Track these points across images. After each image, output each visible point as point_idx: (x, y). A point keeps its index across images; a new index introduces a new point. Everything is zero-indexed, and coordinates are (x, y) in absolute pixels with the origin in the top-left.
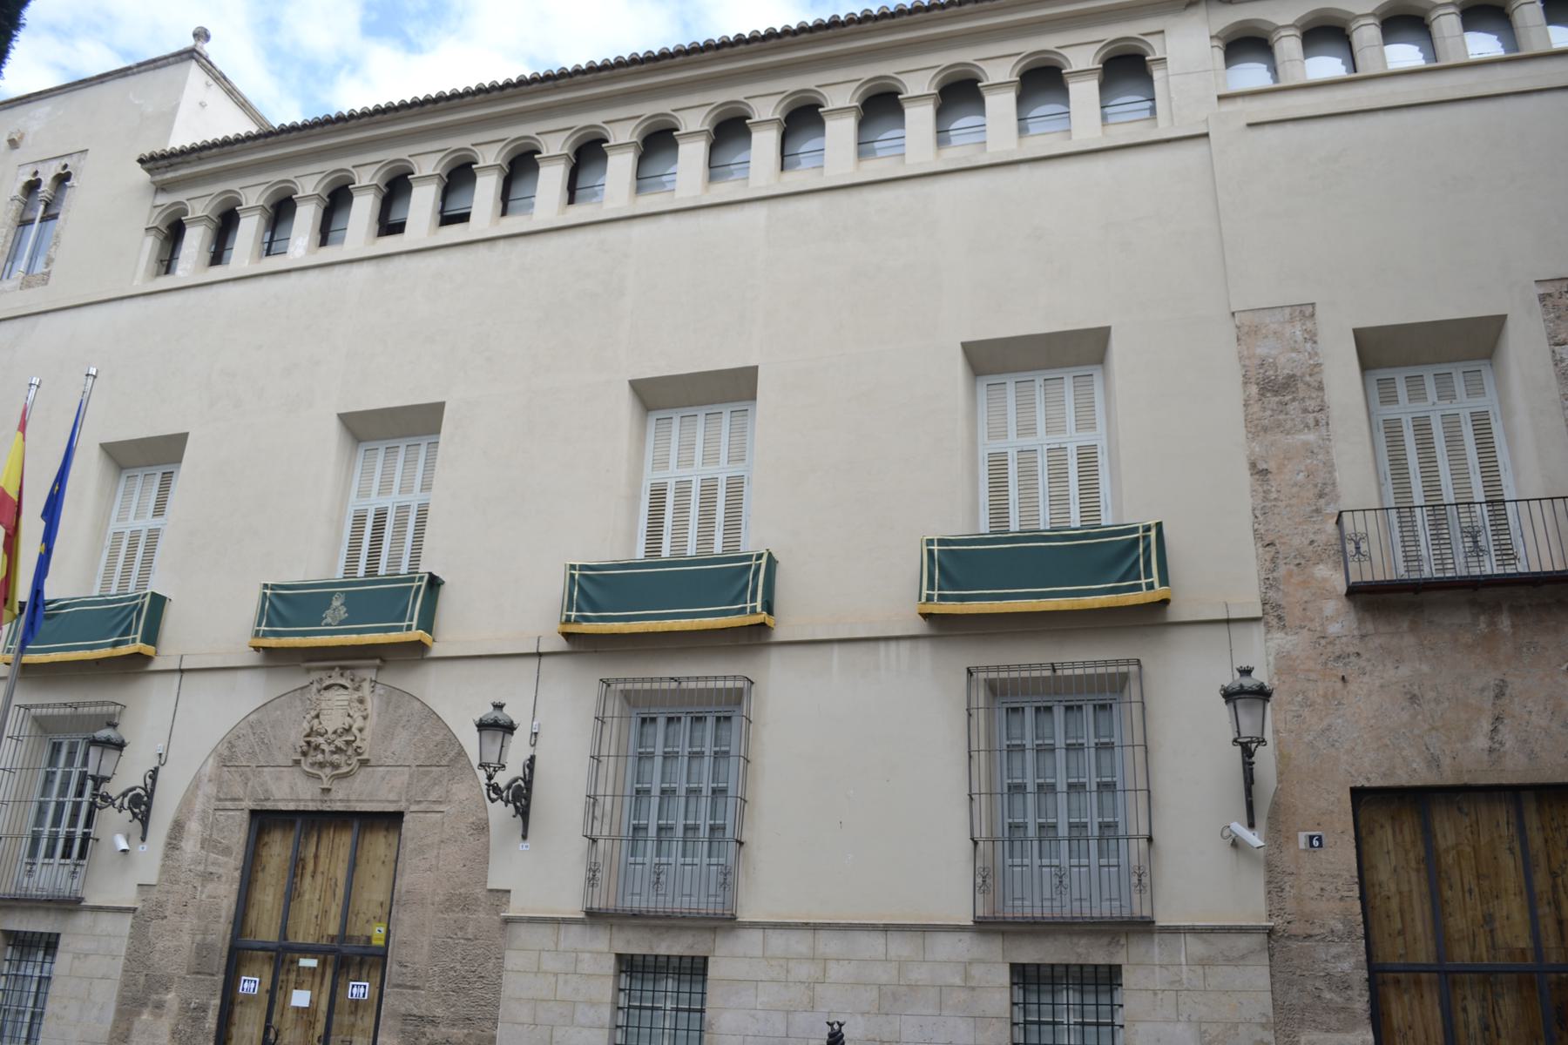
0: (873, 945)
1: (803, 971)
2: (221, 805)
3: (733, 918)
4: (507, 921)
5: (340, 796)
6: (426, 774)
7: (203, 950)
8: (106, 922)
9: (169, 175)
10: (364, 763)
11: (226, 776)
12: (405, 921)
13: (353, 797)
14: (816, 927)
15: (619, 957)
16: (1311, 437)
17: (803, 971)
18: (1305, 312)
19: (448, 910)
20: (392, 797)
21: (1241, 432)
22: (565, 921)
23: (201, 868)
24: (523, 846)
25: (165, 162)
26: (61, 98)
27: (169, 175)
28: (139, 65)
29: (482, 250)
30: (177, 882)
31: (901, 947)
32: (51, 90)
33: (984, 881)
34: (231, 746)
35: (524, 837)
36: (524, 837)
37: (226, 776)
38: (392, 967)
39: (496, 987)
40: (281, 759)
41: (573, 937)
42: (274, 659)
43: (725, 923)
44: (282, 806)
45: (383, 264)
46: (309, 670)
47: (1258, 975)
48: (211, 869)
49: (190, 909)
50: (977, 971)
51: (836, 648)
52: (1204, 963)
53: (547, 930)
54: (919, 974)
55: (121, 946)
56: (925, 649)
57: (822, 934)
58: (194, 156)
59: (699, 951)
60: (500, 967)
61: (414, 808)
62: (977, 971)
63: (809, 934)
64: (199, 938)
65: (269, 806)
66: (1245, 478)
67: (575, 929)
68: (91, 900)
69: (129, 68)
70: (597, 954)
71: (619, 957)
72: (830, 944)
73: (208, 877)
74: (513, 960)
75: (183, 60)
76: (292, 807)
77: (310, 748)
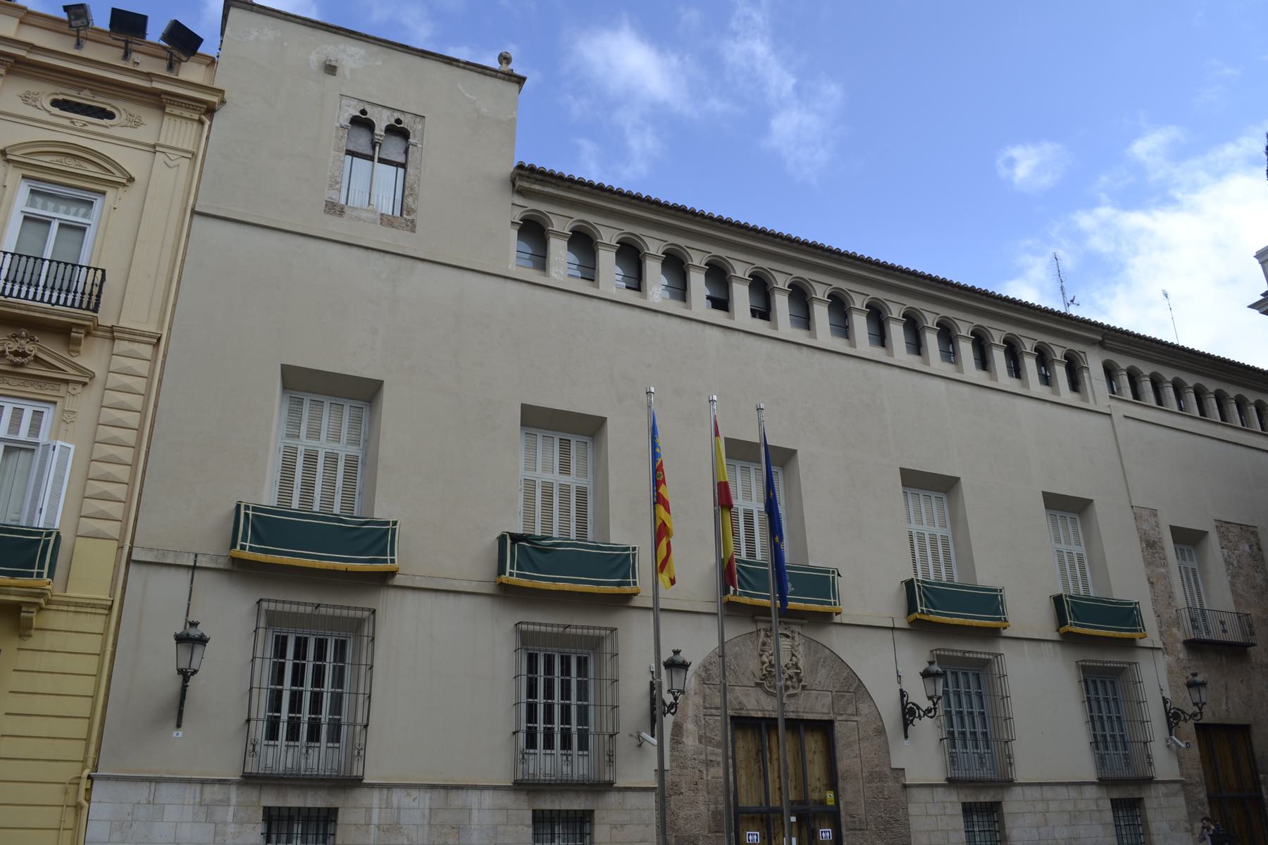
0: (1062, 791)
1: (1040, 806)
2: (709, 712)
3: (1012, 781)
4: (905, 786)
5: (792, 709)
6: (843, 697)
7: (715, 814)
8: (633, 800)
9: (537, 187)
10: (804, 687)
11: (708, 691)
12: (849, 790)
13: (801, 710)
14: (1041, 784)
15: (964, 804)
16: (1163, 570)
17: (1040, 806)
18: (1154, 513)
19: (871, 781)
20: (825, 710)
21: (1142, 565)
22: (937, 786)
23: (703, 757)
24: (906, 743)
25: (540, 177)
26: (375, 48)
27: (537, 187)
28: (468, 63)
29: (779, 345)
30: (685, 767)
31: (1073, 793)
32: (366, 36)
33: (1101, 762)
34: (706, 670)
35: (906, 737)
36: (906, 737)
37: (708, 691)
38: (844, 819)
39: (907, 826)
40: (746, 682)
41: (940, 794)
42: (732, 610)
43: (1009, 783)
44: (753, 714)
45: (728, 333)
46: (756, 622)
47: (1181, 801)
48: (710, 758)
49: (700, 787)
50: (1100, 802)
51: (1025, 644)
52: (1166, 796)
53: (926, 791)
54: (1082, 806)
55: (652, 816)
56: (1058, 647)
57: (1045, 788)
58: (568, 184)
59: (997, 799)
60: (907, 814)
61: (839, 718)
62: (1100, 802)
63: (1039, 788)
64: (712, 807)
65: (744, 713)
66: (1147, 585)
67: (940, 790)
68: (620, 783)
69: (457, 61)
70: (952, 802)
71: (964, 804)
72: (1049, 793)
73: (709, 763)
74: (913, 809)
75: (509, 80)
76: (760, 715)
77: (768, 675)
